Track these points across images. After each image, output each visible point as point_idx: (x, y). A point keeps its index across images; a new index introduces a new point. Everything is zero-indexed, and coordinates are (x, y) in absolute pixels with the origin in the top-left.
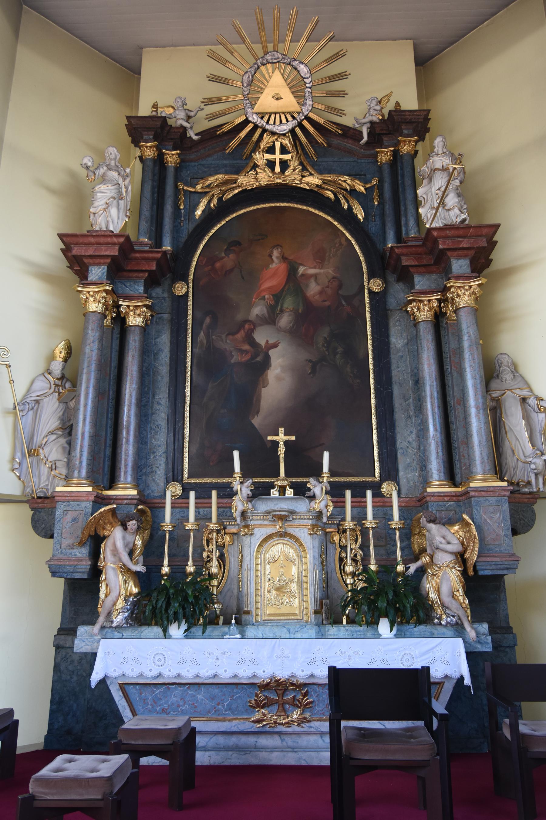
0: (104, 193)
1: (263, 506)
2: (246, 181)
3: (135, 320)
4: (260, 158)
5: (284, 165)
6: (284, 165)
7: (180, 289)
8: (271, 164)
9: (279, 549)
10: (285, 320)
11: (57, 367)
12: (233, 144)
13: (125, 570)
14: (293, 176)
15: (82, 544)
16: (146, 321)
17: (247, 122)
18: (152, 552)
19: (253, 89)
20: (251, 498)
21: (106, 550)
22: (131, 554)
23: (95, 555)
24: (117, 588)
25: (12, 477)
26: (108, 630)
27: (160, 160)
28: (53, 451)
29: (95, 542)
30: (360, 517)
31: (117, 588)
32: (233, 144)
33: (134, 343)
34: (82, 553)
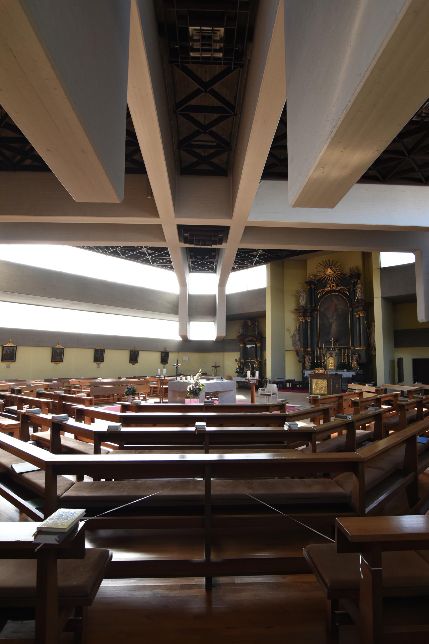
0: (301, 298)
1: (328, 352)
2: (326, 290)
3: (309, 321)
4: (328, 286)
5: (333, 286)
6: (333, 286)
7: (316, 313)
8: (330, 286)
9: (330, 358)
10: (335, 318)
11: (298, 329)
12: (324, 281)
13: (309, 362)
14: (335, 288)
15: (302, 358)
16: (311, 320)
17: (325, 277)
18: (313, 359)
19: (325, 271)
20: (326, 351)
21: (306, 359)
22: (309, 360)
23: (304, 360)
24: (308, 364)
25: (293, 347)
26: (307, 370)
27: (311, 288)
28: (298, 343)
29: (304, 358)
30: (344, 353)
31: (308, 364)
32: (324, 281)
33: (309, 324)
34: (303, 359)
